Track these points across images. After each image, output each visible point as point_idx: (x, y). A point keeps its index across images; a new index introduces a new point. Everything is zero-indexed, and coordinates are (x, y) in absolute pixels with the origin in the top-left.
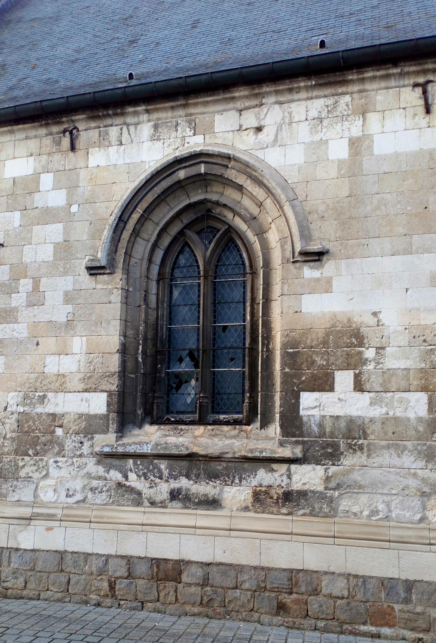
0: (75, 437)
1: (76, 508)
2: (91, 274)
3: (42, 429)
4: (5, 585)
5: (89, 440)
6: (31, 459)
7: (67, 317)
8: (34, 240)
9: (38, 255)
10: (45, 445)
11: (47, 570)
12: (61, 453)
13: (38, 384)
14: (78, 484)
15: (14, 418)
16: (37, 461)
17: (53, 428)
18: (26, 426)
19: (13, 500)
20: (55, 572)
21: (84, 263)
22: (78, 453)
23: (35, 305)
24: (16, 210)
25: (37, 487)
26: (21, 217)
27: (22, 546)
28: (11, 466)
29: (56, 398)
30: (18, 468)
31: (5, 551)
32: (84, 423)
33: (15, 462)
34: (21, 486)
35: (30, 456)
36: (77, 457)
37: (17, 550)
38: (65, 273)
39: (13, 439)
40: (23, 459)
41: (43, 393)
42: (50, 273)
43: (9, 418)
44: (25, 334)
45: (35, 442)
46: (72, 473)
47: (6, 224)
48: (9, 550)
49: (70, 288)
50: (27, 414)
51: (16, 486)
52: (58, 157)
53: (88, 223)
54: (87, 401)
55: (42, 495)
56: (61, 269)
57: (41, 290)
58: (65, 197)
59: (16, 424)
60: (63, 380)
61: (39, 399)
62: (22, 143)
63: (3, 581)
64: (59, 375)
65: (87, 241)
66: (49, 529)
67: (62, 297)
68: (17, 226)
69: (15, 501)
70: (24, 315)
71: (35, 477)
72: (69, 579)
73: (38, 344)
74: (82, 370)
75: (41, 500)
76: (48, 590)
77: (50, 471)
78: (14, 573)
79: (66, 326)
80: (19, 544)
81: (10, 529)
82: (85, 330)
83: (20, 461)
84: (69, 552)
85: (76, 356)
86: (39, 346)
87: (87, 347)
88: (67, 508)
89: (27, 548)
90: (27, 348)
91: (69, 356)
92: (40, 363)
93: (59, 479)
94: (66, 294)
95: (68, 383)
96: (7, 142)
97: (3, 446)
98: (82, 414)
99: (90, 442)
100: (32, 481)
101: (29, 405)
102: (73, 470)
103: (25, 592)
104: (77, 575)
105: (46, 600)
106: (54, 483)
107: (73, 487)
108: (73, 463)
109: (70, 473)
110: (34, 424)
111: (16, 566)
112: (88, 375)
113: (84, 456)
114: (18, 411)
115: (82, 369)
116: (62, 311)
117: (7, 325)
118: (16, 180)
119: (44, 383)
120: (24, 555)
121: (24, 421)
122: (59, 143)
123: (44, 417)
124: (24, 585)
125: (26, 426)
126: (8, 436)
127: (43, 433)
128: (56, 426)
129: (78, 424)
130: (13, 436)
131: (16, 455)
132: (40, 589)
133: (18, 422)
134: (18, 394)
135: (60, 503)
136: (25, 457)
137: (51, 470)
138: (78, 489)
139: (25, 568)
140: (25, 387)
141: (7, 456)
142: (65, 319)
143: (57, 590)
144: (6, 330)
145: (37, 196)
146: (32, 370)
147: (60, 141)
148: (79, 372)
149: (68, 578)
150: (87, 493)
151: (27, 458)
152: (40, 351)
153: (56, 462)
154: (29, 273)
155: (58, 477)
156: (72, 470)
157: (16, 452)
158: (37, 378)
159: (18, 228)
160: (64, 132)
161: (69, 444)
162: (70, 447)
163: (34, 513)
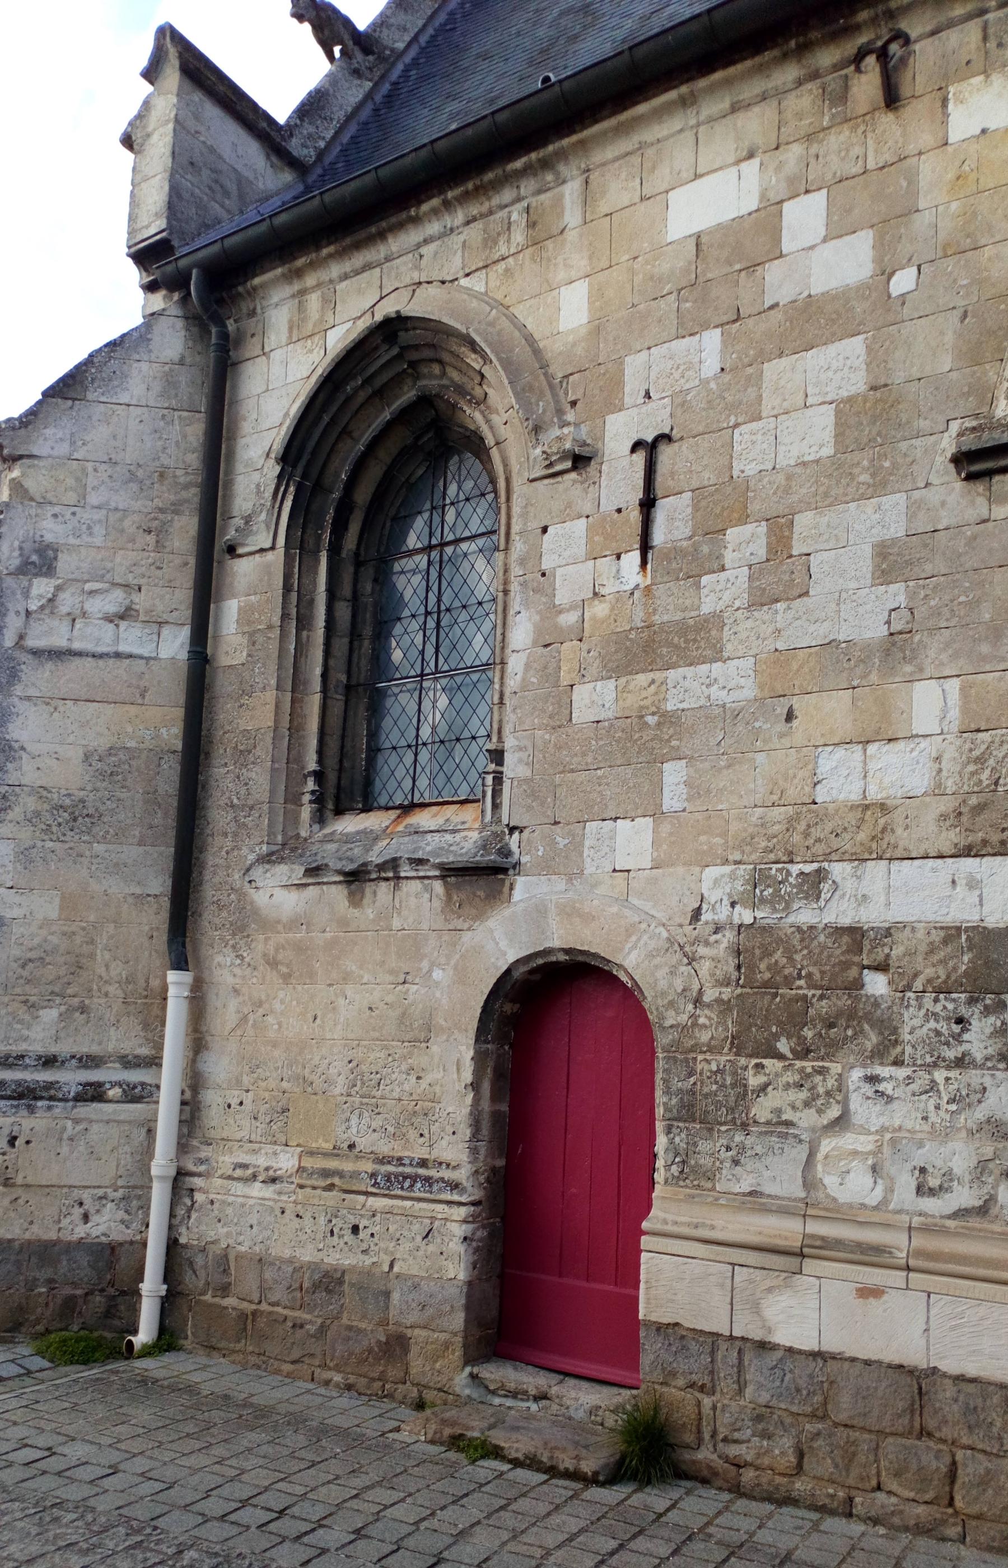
0: (936, 1000)
1: (957, 1234)
3: (817, 976)
4: (733, 1451)
5: (987, 1011)
6: (786, 1068)
7: (888, 622)
8: (769, 404)
9: (781, 449)
10: (831, 1026)
11: (872, 1422)
13: (797, 838)
16: (808, 1076)
17: (854, 972)
19: (737, 1190)
20: (901, 1435)
22: (950, 1054)
24: (705, 326)
26: (724, 342)
27: (782, 1337)
28: (724, 1086)
29: (859, 878)
30: (745, 1094)
31: (723, 1346)
32: (966, 959)
33: (735, 1074)
34: (759, 1149)
35: (781, 1057)
36: (948, 1068)
37: (763, 1346)
39: (724, 1006)
40: (759, 1066)
41: (815, 866)
43: (707, 944)
44: (749, 691)
46: (933, 1118)
47: (677, 375)
48: (738, 1344)
50: (766, 930)
51: (742, 1148)
52: (842, 138)
54: (973, 884)
55: (830, 1181)
57: (795, 553)
59: (732, 962)
60: (882, 822)
61: (801, 885)
62: (719, 127)
63: (725, 1440)
64: (867, 807)
66: (869, 1292)
67: (869, 562)
68: (710, 374)
69: (744, 1195)
71: (803, 1124)
73: (790, 717)
75: (828, 1196)
76: (879, 1488)
77: (852, 1107)
78: (759, 1418)
80: (770, 1330)
81: (737, 1279)
83: (751, 1072)
84: (945, 1375)
85: (924, 744)
86: (795, 723)
88: (926, 1229)
90: (757, 733)
92: (801, 774)
95: (899, 831)
96: (672, 135)
97: (695, 1024)
98: (958, 929)
99: (992, 1019)
100: (796, 1136)
101: (771, 902)
102: (937, 1107)
105: (876, 1521)
106: (870, 1147)
107: (939, 1163)
108: (933, 1087)
109: (925, 1118)
110: (790, 959)
111: (764, 1397)
113: (973, 1064)
114: (736, 921)
115: (949, 783)
116: (868, 607)
117: (689, 671)
118: (704, 239)
119: (816, 833)
120: (789, 1365)
121: (757, 952)
122: (842, 96)
123: (822, 938)
124: (793, 1459)
125: (763, 966)
127: (821, 988)
128: (864, 967)
129: (943, 962)
130: (725, 997)
131: (737, 1054)
132: (851, 1482)
133: (739, 953)
134: (733, 872)
135: (899, 1212)
136: (766, 1062)
137: (856, 1103)
138: (957, 1171)
139: (794, 1409)
140: (755, 850)
141: (708, 1056)
142: (884, 631)
143: (912, 1495)
144: (687, 684)
145: (773, 273)
146: (775, 798)
147: (846, 88)
150: (995, 1187)
151: (771, 1064)
152: (798, 739)
153: (872, 1079)
155: (883, 1130)
156: (931, 1108)
157: (738, 1044)
158: (791, 823)
159: (715, 377)
160: (858, 59)
163: (813, 1236)
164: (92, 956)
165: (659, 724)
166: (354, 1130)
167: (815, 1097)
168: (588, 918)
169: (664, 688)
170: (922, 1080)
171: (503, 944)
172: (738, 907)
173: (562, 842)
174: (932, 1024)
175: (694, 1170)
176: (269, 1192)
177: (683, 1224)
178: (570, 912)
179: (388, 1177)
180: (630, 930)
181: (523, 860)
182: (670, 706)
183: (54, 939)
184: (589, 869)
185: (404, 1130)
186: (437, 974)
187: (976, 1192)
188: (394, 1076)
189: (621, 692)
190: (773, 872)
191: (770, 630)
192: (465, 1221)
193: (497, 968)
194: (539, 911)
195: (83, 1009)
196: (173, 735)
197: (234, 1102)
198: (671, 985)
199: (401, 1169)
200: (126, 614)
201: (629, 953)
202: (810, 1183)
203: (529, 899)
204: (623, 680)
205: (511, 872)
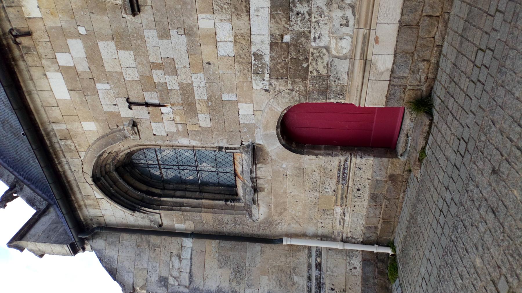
0: (292, 21)
1: (360, 15)
2: (139, 11)
3: (285, 55)
4: (423, 80)
5: (295, 6)
6: (311, 65)
10: (299, 51)
11: (415, 40)
12: (306, 35)
13: (244, 61)
14: (337, 14)
15: (275, 83)
16: (314, 58)
17: (283, 45)
18: (282, 71)
19: (347, 79)
20: (418, 31)
21: (130, 17)
22: (307, 17)
23: (175, 67)
25: (337, 57)
27: (390, 66)
28: (316, 83)
29: (256, 43)
30: (319, 76)
31: (392, 83)
32: (279, 12)
33: (313, 79)
34: (335, 72)
35: (308, 66)
36: (311, 17)
37: (392, 71)
38: (142, 37)
39: (293, 83)
41: (252, 56)
42: (144, 53)
43: (275, 88)
44: (201, 75)
45: (297, 62)
46: (326, 22)
48: (392, 79)
49: (154, 32)
51: (335, 77)
53: (91, 15)
55: (344, 52)
56: (139, 42)
58: (74, 40)
59: (280, 80)
60: (239, 37)
61: (258, 60)
63: (420, 82)
64: (235, 41)
65: (109, 16)
69: (348, 77)
70: (185, 77)
71: (328, 60)
72: (427, 16)
73: (209, 63)
74: (229, 17)
75: (349, 52)
76: (434, 38)
77: (323, 45)
78: (414, 72)
79: (190, 35)
81: (373, 79)
82: (191, 15)
83: (313, 75)
84: (401, 18)
86: (211, 62)
87: (207, 12)
88: (358, 24)
89: (392, 61)
90: (214, 73)
91: (217, 31)
92: (226, 60)
93: (331, 35)
94: (161, 37)
97: (299, 91)
98: (271, 14)
99: (297, 5)
100: (331, 62)
101: (263, 69)
102: (323, 21)
103: (433, 60)
104: (425, 8)
105: (444, 39)
106: (334, 40)
107: (339, 20)
109: (326, 24)
110: (280, 63)
111: (407, 71)
112: (233, 10)
113: (310, 10)
114: (268, 79)
117: (196, 93)
119: (243, 56)
120: (398, 64)
121: (277, 73)
123: (273, 54)
124: (426, 62)
125: (282, 71)
126: (290, 87)
127: (288, 54)
128: (282, 42)
130: (291, 82)
131: (307, 79)
132: (432, 46)
135: (353, 32)
136: (310, 70)
137: (322, 44)
139: (411, 62)
141: (308, 87)
143: (436, 28)
144: (199, 93)
148: (231, 20)
149: (426, 18)
152: (215, 61)
153: (315, 39)
154: (148, 74)
155: (329, 36)
156: (323, 22)
157: (305, 79)
158: (240, 63)
161: (299, 27)
162: (301, 26)
163: (360, 57)
164: (279, 266)
165: (211, 102)
166: (330, 190)
167: (320, 56)
168: (268, 122)
169: (200, 100)
170: (315, 25)
171: (275, 147)
172: (265, 79)
173: (245, 130)
174: (299, 22)
175: (341, 91)
176: (347, 215)
177: (357, 95)
178: (266, 128)
179: (343, 180)
180: (271, 110)
181: (251, 141)
182: (206, 98)
183: (274, 277)
184: (253, 122)
185: (329, 176)
186: (284, 166)
187: (347, 10)
188: (314, 179)
189: (202, 113)
190: (254, 68)
191: (184, 69)
192: (356, 158)
193: (282, 149)
194: (266, 136)
195: (294, 269)
196: (214, 243)
197: (321, 225)
198: (287, 98)
199: (341, 177)
200: (179, 257)
201: (278, 110)
202: (345, 58)
203: (262, 139)
204: (198, 112)
205: (254, 144)
